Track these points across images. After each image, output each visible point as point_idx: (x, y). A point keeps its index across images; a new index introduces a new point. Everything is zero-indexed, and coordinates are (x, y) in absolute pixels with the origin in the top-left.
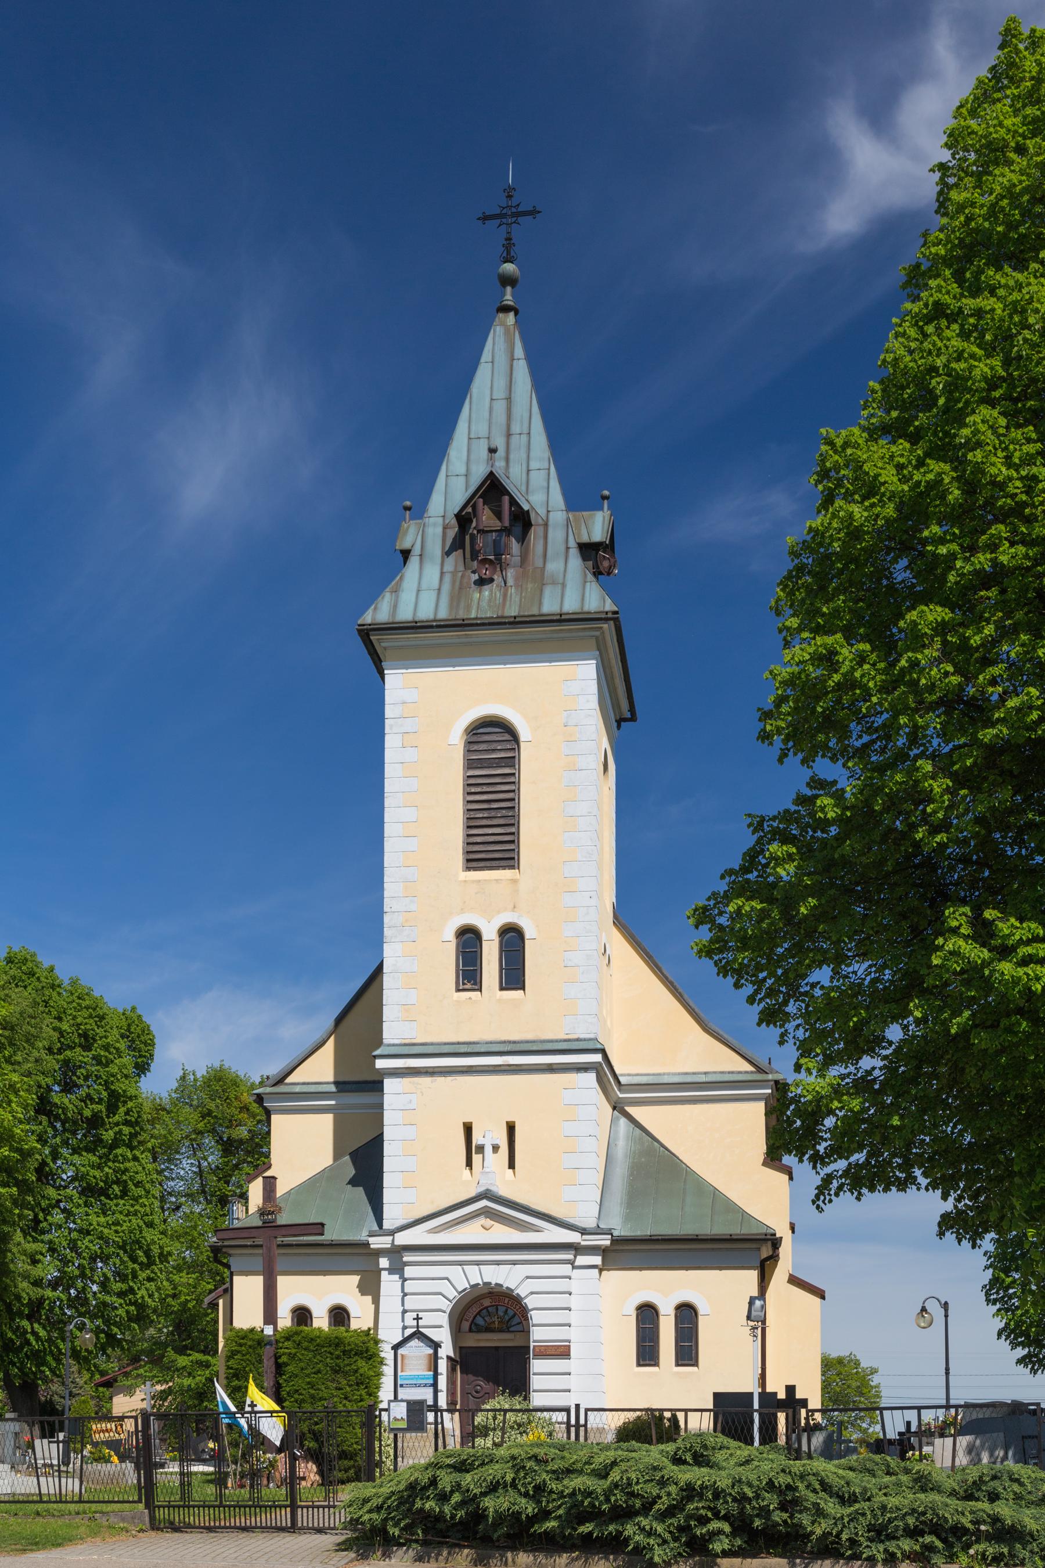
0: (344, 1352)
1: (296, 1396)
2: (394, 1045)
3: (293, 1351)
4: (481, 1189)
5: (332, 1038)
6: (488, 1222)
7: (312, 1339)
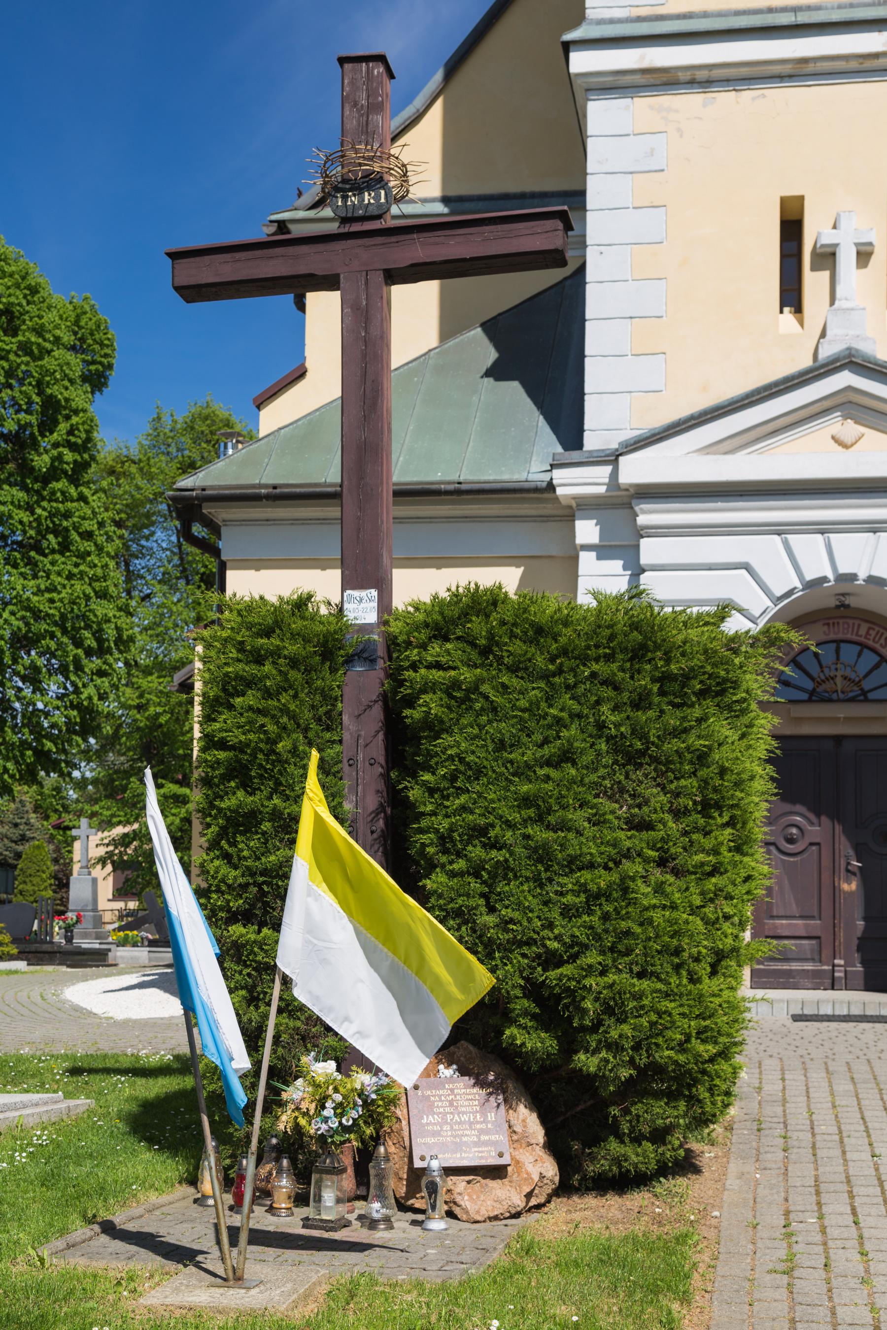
0: (664, 679)
1: (476, 851)
2: (612, 21)
3: (466, 675)
4: (827, 351)
5: (438, 105)
6: (849, 429)
7: (540, 630)
